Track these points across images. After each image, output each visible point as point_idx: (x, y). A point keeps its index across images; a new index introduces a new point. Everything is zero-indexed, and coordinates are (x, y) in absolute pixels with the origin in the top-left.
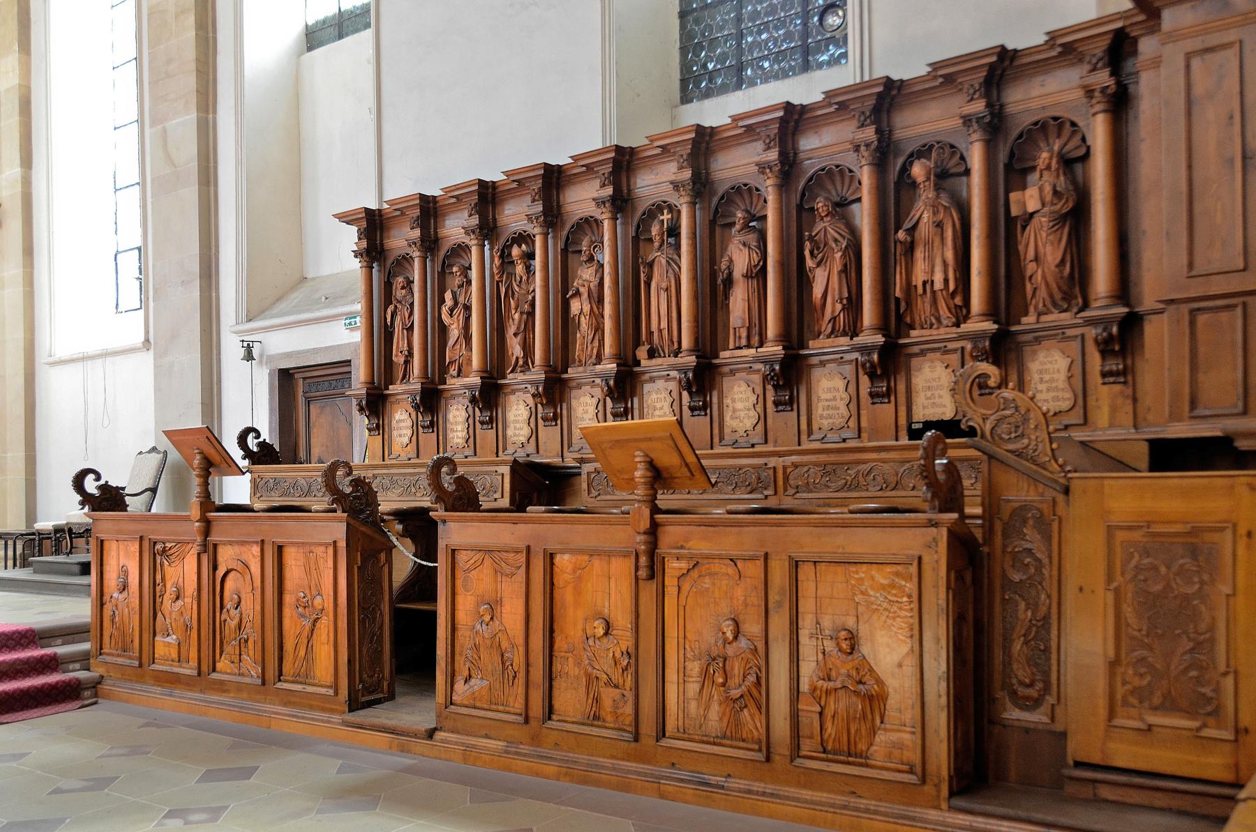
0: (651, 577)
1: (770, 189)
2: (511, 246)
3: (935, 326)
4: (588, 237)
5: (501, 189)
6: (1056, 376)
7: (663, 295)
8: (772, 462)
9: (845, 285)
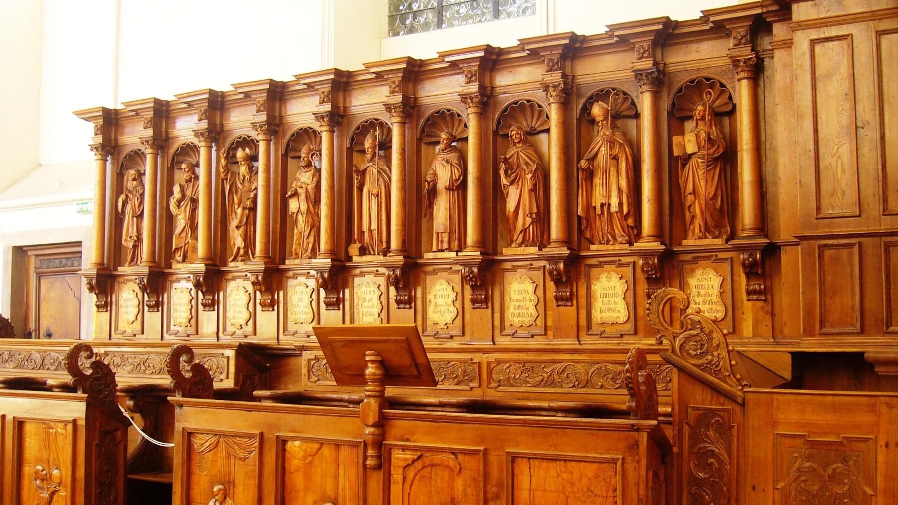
0: (379, 467)
1: (471, 116)
2: (236, 148)
3: (611, 243)
4: (306, 145)
6: (711, 291)
7: (374, 202)
8: (478, 358)
9: (535, 202)
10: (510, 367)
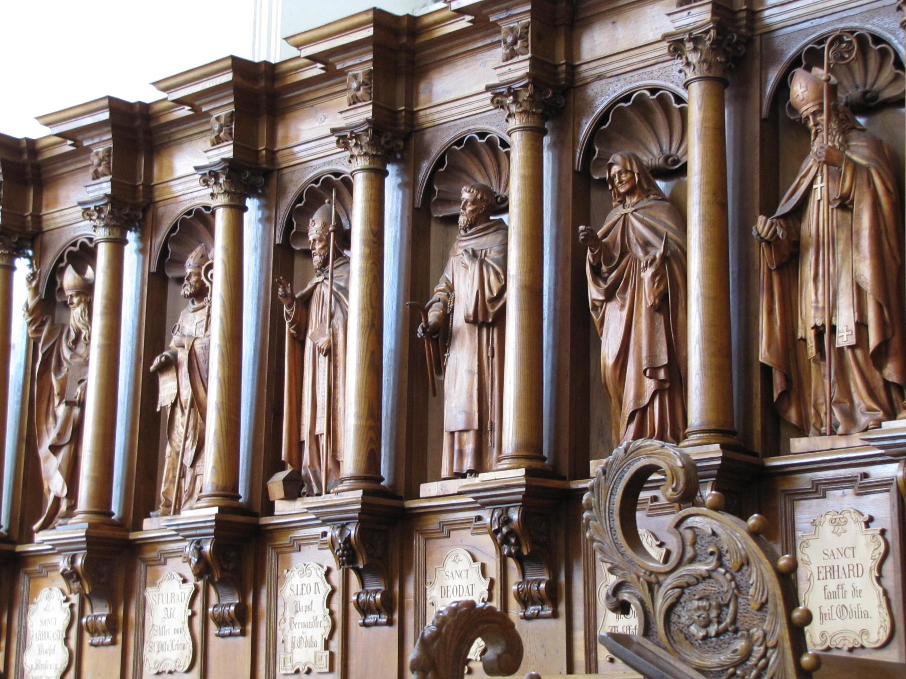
2: (63, 270)
3: (840, 430)
4: (198, 249)
5: (48, 154)
7: (323, 362)
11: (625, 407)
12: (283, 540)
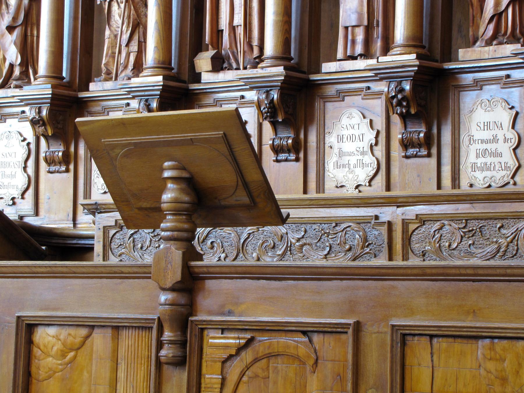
10: (441, 228)
11: (486, 12)
12: (207, 101)
